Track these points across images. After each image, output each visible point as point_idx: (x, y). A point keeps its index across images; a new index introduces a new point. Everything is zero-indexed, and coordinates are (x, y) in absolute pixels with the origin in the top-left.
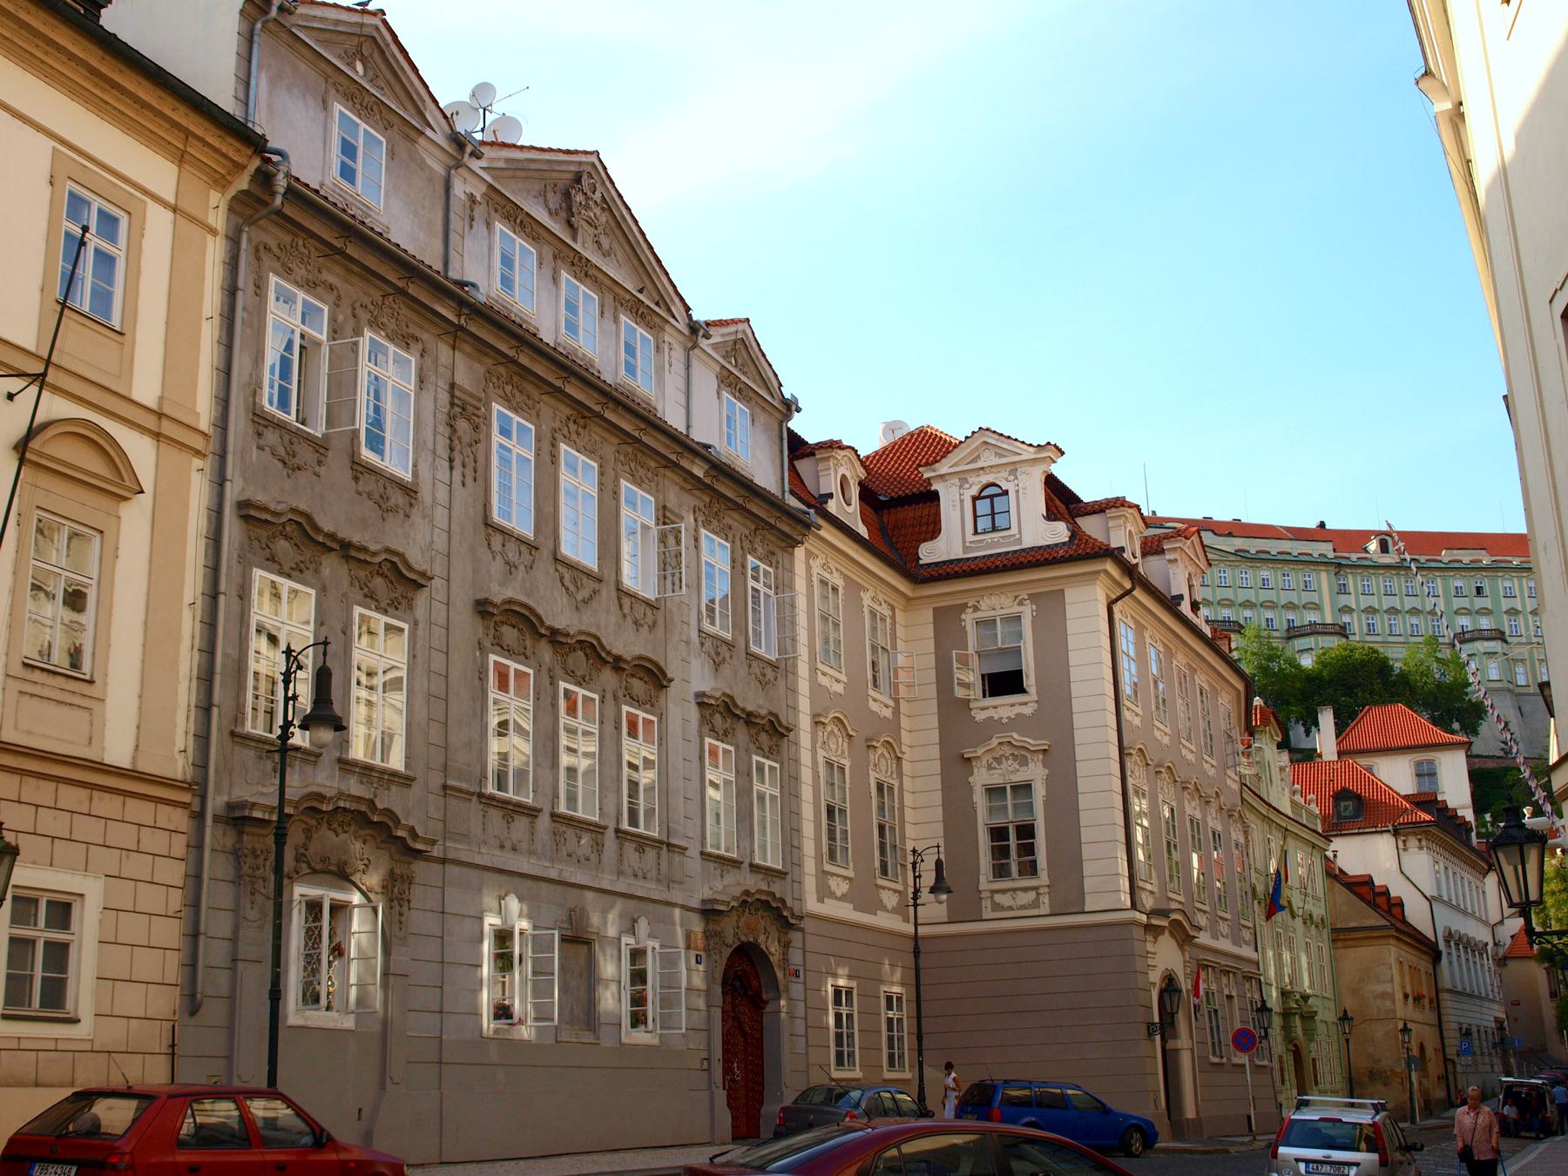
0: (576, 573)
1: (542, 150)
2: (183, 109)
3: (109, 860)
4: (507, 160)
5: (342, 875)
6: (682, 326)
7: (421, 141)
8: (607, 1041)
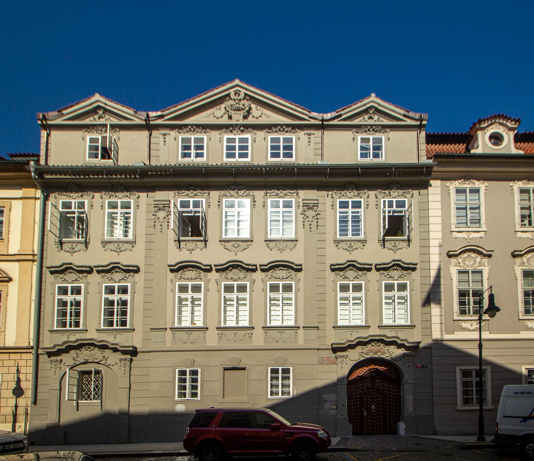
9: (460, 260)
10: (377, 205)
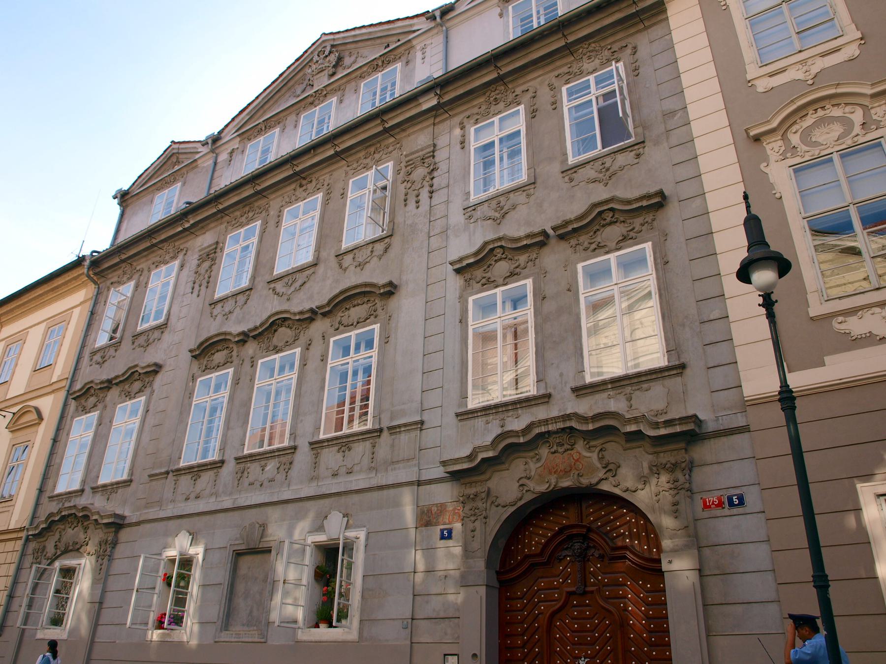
0: (286, 280)
1: (270, 86)
2: (70, 273)
4: (248, 114)
7: (199, 162)
8: (276, 639)
9: (795, 139)
10: (554, 103)
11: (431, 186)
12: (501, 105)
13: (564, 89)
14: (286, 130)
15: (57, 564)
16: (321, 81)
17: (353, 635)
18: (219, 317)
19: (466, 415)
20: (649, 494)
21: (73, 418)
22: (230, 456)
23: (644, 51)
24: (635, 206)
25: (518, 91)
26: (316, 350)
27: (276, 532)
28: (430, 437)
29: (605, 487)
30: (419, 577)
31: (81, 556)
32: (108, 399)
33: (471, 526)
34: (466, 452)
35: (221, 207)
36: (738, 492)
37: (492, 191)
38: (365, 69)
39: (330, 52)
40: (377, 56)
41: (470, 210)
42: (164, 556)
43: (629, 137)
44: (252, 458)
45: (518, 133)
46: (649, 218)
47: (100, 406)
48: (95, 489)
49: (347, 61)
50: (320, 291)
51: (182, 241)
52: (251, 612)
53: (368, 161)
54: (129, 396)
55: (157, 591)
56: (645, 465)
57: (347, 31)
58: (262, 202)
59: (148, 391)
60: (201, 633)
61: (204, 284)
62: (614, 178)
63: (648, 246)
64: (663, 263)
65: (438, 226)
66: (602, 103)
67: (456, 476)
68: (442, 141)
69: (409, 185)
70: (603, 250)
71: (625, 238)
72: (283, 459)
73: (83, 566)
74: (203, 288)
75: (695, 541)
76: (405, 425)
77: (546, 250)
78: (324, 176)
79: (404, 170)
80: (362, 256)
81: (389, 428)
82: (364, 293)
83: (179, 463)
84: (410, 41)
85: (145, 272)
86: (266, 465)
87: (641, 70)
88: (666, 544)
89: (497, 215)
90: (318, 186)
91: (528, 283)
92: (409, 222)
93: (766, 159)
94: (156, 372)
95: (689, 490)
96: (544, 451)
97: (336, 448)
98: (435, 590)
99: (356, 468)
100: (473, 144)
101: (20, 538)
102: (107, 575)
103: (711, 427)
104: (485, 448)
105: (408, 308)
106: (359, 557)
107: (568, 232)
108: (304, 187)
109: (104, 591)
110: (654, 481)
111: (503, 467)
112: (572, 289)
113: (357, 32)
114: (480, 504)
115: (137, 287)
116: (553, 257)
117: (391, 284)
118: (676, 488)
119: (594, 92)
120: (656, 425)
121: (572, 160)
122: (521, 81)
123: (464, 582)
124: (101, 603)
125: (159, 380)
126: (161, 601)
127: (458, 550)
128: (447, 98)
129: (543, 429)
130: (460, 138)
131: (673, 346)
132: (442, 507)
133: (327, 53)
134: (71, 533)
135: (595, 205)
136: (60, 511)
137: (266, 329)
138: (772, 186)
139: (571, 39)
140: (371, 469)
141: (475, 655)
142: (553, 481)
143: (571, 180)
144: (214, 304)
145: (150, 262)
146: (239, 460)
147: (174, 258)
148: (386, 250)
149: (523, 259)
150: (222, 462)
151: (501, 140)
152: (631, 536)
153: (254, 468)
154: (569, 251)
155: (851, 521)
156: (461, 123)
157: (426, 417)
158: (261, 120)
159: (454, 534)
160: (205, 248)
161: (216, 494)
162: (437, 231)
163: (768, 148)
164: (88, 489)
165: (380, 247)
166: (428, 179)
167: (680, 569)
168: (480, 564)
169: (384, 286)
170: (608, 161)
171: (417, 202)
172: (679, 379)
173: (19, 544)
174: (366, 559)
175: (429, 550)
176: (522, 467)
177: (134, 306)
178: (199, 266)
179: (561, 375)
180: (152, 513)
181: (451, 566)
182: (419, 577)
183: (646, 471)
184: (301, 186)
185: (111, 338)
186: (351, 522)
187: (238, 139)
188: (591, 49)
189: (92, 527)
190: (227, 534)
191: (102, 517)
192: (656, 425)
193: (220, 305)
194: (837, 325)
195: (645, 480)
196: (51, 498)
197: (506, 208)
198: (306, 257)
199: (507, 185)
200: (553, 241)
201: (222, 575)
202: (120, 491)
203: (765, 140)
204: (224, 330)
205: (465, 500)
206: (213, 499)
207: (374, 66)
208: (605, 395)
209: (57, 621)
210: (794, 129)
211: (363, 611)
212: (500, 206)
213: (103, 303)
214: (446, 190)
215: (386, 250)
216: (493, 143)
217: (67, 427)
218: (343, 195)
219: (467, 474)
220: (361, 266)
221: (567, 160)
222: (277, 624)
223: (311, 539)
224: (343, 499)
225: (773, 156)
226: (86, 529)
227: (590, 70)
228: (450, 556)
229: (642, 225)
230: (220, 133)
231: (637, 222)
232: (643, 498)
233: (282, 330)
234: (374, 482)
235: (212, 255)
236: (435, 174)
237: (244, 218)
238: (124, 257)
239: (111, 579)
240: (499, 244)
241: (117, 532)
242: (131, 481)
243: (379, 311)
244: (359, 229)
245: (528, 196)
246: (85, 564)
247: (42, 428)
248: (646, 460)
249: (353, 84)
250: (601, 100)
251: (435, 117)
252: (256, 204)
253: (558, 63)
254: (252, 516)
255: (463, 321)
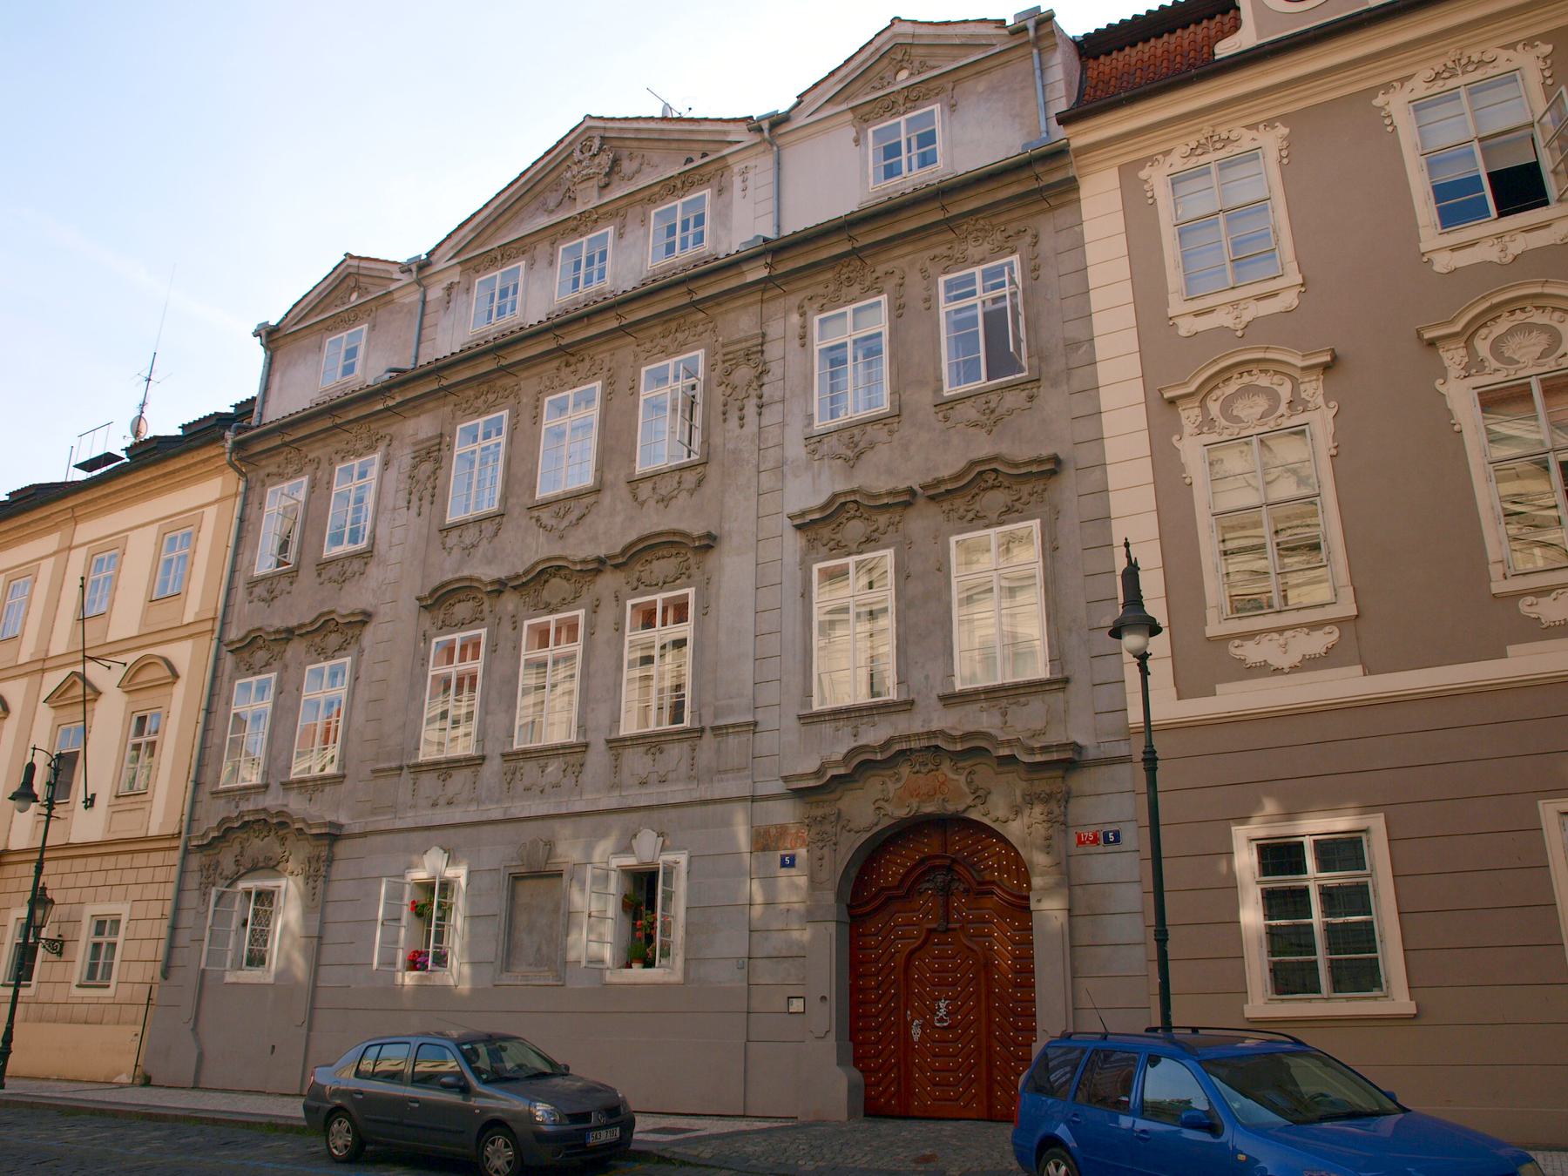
0: (555, 508)
3: (135, 892)
5: (271, 867)
6: (749, 139)
7: (396, 295)
9: (1214, 408)
10: (927, 300)
11: (760, 397)
12: (856, 288)
13: (942, 280)
14: (536, 267)
15: (242, 885)
16: (589, 199)
17: (676, 976)
18: (456, 553)
19: (810, 719)
20: (1022, 828)
21: (232, 679)
22: (494, 750)
23: (1046, 245)
24: (1023, 470)
25: (881, 270)
26: (607, 615)
27: (568, 852)
28: (765, 742)
29: (974, 815)
30: (757, 911)
31: (280, 875)
32: (289, 654)
33: (818, 853)
34: (812, 765)
35: (445, 383)
36: (1115, 828)
37: (843, 419)
38: (657, 189)
39: (600, 149)
40: (675, 173)
41: (814, 441)
42: (408, 879)
43: (1021, 370)
44: (526, 755)
45: (880, 334)
46: (1039, 487)
47: (276, 664)
48: (287, 786)
49: (627, 166)
50: (611, 531)
51: (382, 423)
52: (539, 949)
53: (667, 341)
54: (324, 653)
55: (404, 922)
56: (1018, 793)
57: (626, 119)
58: (509, 381)
59: (354, 649)
60: (474, 976)
61: (427, 498)
62: (1000, 424)
63: (1035, 524)
64: (1051, 549)
65: (772, 456)
66: (990, 307)
67: (799, 793)
68: (774, 329)
69: (729, 391)
70: (982, 522)
71: (1009, 510)
72: (572, 759)
73: (283, 889)
74: (426, 503)
75: (1068, 881)
76: (734, 726)
77: (912, 513)
78: (602, 354)
79: (719, 367)
80: (665, 487)
81: (713, 729)
82: (672, 543)
83: (417, 756)
84: (723, 157)
85: (324, 464)
86: (547, 766)
87: (1041, 272)
88: (1037, 882)
89: (849, 453)
90: (594, 370)
91: (888, 555)
92: (730, 446)
93: (1179, 430)
94: (364, 623)
95: (1064, 823)
96: (905, 770)
97: (642, 749)
98: (775, 925)
99: (670, 776)
100: (818, 345)
101: (176, 848)
102: (325, 902)
103: (1092, 754)
104: (837, 764)
105: (734, 569)
106: (681, 886)
107: (939, 494)
108: (572, 368)
109: (323, 923)
110: (1027, 812)
111: (856, 785)
112: (943, 568)
113: (642, 125)
114: (828, 828)
115: (313, 486)
116: (920, 522)
117: (709, 535)
118: (1051, 821)
119: (980, 300)
120: (1031, 751)
121: (948, 391)
122: (883, 257)
123: (810, 917)
124: (320, 938)
125: (369, 635)
126: (406, 936)
127: (803, 881)
128: (780, 269)
129: (904, 746)
130: (799, 330)
131: (1057, 657)
132: (782, 830)
133: (595, 149)
134: (258, 845)
135: (973, 464)
136: (241, 815)
137: (532, 579)
138: (1182, 468)
139: (954, 211)
140: (690, 778)
141: (823, 998)
142: (915, 806)
143: (946, 419)
144: (446, 530)
145: (330, 449)
146: (507, 757)
147: (371, 448)
148: (699, 483)
149: (882, 519)
150: (483, 758)
151: (855, 342)
152: (999, 869)
153: (530, 769)
154: (941, 517)
155: (1223, 867)
156: (801, 307)
157: (758, 718)
158: (495, 245)
159: (797, 861)
160: (422, 442)
161: (479, 802)
162: (770, 465)
163: (1184, 415)
164: (274, 785)
165: (690, 478)
166: (755, 385)
167: (1049, 910)
168: (829, 897)
169: (700, 538)
170: (994, 397)
171: (741, 419)
172: (1061, 694)
173: (175, 857)
174: (689, 888)
175: (768, 881)
176: (880, 787)
177: (313, 516)
178: (415, 467)
179: (927, 677)
180: (384, 822)
181: (795, 899)
182: (757, 911)
183: (1019, 800)
184: (568, 365)
185: (280, 563)
186: (668, 842)
187: (459, 268)
188: (978, 227)
189: (291, 838)
190: (499, 852)
191: (309, 826)
192: (1031, 751)
193: (456, 533)
194: (1235, 650)
195: (1017, 812)
196: (216, 794)
197: (862, 445)
198: (584, 478)
199: (864, 414)
200: (921, 501)
201: (498, 904)
202: (327, 789)
203: (1181, 405)
204: (466, 573)
205: (813, 822)
206: (473, 807)
207: (671, 187)
208: (976, 707)
209: (257, 959)
210: (1214, 395)
211: (687, 950)
212: (853, 443)
213: (256, 506)
214: (779, 407)
215: (699, 483)
216: (845, 345)
217: (225, 693)
218: (634, 390)
219: (814, 793)
220: (665, 501)
221: (941, 389)
222: (584, 964)
223: (615, 862)
224: (656, 814)
225: (1189, 428)
226: (283, 840)
227: (977, 258)
228: (794, 887)
229: (1031, 495)
230: (429, 254)
231: (1026, 489)
232: (1015, 830)
233: (554, 581)
234: (696, 796)
235: (434, 453)
236: (766, 379)
237: (480, 401)
238: (288, 439)
239: (330, 908)
240: (853, 498)
241: (331, 846)
242: (344, 776)
243: (694, 570)
244: (660, 445)
245: (891, 432)
246: (290, 890)
247: (179, 689)
248: (1019, 787)
249: (638, 209)
250: (989, 304)
251: (764, 291)
252: (499, 383)
253: (934, 239)
254: (531, 831)
255: (806, 594)
